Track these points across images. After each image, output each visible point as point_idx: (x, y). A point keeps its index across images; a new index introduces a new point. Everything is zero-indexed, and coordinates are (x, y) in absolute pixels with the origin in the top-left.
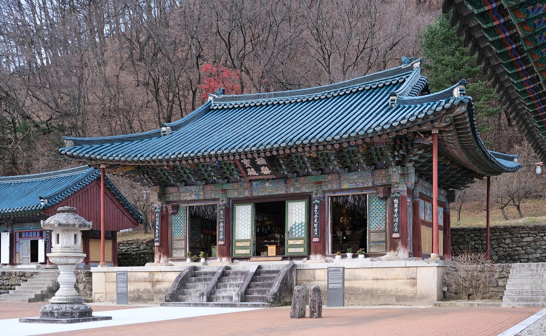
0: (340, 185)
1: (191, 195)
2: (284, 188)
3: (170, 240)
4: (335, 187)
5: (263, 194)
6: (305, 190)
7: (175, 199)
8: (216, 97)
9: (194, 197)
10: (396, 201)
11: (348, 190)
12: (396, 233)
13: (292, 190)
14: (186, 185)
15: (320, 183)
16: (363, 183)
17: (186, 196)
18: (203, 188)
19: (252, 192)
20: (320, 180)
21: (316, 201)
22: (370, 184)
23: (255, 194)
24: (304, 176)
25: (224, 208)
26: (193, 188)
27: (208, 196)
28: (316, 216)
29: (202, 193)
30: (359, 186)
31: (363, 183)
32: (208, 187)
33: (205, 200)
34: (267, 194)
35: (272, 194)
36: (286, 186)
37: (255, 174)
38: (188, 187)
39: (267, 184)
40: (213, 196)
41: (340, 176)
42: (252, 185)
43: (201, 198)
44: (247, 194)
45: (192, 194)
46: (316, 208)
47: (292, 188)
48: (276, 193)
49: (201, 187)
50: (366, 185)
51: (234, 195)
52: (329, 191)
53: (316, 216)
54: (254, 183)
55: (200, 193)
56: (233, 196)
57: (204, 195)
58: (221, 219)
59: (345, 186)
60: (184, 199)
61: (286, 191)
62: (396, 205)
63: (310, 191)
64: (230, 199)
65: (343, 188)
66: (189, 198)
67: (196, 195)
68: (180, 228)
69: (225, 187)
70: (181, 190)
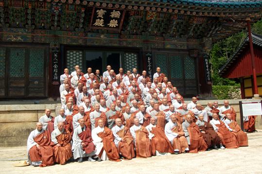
0: (164, 45)
4: (160, 46)
5: (96, 45)
11: (169, 49)
13: (125, 44)
14: (9, 27)
17: (11, 37)
21: (149, 54)
24: (133, 34)
26: (21, 31)
28: (149, 65)
30: (178, 48)
35: (107, 45)
38: (15, 29)
40: (43, 40)
42: (86, 35)
43: (30, 41)
44: (80, 42)
45: (18, 35)
48: (110, 45)
49: (30, 31)
50: (182, 48)
53: (149, 65)
54: (89, 34)
62: (207, 63)
63: (141, 46)
64: (61, 45)
67: (21, 38)
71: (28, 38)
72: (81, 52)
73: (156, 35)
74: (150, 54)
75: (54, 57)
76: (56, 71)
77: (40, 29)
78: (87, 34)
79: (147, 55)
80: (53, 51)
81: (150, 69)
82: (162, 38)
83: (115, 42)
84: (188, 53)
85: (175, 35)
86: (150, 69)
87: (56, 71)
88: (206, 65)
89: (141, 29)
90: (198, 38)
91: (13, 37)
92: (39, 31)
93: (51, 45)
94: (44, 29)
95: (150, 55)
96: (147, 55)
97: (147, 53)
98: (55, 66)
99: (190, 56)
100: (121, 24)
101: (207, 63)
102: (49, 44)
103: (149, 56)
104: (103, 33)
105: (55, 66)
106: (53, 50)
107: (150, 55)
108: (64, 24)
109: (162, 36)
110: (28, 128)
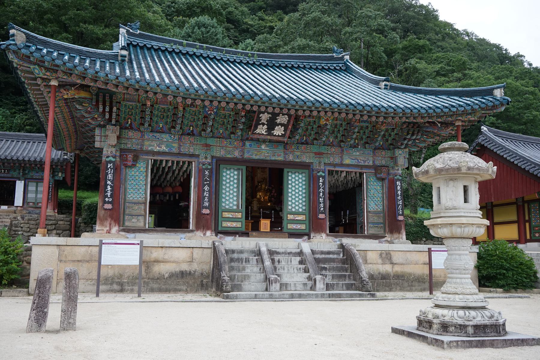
1: (161, 145)
2: (282, 154)
3: (122, 201)
4: (337, 161)
5: (257, 157)
6: (306, 159)
7: (135, 147)
8: (131, 31)
9: (164, 148)
10: (398, 183)
11: (348, 166)
12: (401, 215)
13: (291, 158)
15: (322, 154)
16: (365, 161)
17: (153, 146)
18: (179, 139)
19: (244, 153)
20: (323, 151)
21: (321, 173)
22: (371, 163)
23: (246, 156)
24: (302, 143)
25: (209, 167)
26: (165, 137)
27: (183, 150)
28: (321, 190)
29: (176, 145)
30: (360, 164)
31: (365, 161)
32: (187, 140)
33: (179, 154)
34: (262, 158)
35: (268, 158)
36: (284, 152)
37: (264, 132)
38: (158, 135)
39: (263, 147)
41: (343, 151)
42: (244, 145)
43: (174, 150)
44: (237, 154)
46: (321, 181)
47: (291, 155)
48: (273, 158)
49: (177, 137)
50: (366, 164)
51: (220, 153)
52: (330, 164)
53: (321, 190)
55: (174, 145)
56: (218, 155)
57: (179, 148)
58: (206, 180)
59: (347, 161)
60: (150, 148)
61: (285, 157)
62: (399, 188)
63: (311, 161)
64: (213, 157)
65: (344, 163)
66: (157, 149)
67: (167, 146)
68: (138, 187)
69: (210, 141)
70: (146, 137)
71: (174, 147)
72: (236, 173)
73: (332, 145)
74: (323, 172)
75: (204, 175)
76: (207, 195)
77: (189, 134)
78: (245, 143)
79: (318, 174)
80: (204, 167)
81: (321, 194)
82: (340, 149)
83: (278, 155)
84: (374, 171)
85: (358, 144)
86: (321, 194)
87: (207, 195)
88: (397, 191)
89: (313, 136)
90: (389, 150)
91: (156, 145)
92: (187, 137)
93: (200, 157)
94: (193, 135)
95: (323, 174)
96: (318, 174)
97: (319, 172)
98: (206, 188)
99: (376, 175)
100: (288, 132)
101: (399, 188)
102: (198, 156)
103: (321, 176)
104: (264, 141)
105: (206, 188)
106: (203, 165)
107: (323, 174)
108: (217, 129)
109: (340, 146)
110: (182, 269)
